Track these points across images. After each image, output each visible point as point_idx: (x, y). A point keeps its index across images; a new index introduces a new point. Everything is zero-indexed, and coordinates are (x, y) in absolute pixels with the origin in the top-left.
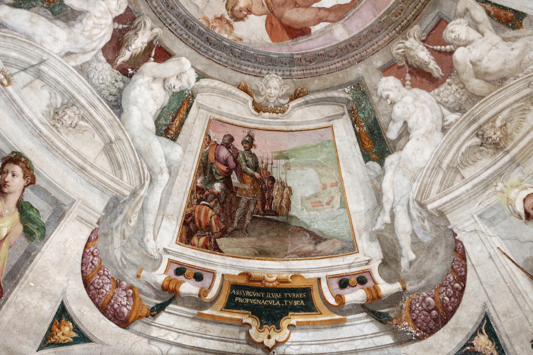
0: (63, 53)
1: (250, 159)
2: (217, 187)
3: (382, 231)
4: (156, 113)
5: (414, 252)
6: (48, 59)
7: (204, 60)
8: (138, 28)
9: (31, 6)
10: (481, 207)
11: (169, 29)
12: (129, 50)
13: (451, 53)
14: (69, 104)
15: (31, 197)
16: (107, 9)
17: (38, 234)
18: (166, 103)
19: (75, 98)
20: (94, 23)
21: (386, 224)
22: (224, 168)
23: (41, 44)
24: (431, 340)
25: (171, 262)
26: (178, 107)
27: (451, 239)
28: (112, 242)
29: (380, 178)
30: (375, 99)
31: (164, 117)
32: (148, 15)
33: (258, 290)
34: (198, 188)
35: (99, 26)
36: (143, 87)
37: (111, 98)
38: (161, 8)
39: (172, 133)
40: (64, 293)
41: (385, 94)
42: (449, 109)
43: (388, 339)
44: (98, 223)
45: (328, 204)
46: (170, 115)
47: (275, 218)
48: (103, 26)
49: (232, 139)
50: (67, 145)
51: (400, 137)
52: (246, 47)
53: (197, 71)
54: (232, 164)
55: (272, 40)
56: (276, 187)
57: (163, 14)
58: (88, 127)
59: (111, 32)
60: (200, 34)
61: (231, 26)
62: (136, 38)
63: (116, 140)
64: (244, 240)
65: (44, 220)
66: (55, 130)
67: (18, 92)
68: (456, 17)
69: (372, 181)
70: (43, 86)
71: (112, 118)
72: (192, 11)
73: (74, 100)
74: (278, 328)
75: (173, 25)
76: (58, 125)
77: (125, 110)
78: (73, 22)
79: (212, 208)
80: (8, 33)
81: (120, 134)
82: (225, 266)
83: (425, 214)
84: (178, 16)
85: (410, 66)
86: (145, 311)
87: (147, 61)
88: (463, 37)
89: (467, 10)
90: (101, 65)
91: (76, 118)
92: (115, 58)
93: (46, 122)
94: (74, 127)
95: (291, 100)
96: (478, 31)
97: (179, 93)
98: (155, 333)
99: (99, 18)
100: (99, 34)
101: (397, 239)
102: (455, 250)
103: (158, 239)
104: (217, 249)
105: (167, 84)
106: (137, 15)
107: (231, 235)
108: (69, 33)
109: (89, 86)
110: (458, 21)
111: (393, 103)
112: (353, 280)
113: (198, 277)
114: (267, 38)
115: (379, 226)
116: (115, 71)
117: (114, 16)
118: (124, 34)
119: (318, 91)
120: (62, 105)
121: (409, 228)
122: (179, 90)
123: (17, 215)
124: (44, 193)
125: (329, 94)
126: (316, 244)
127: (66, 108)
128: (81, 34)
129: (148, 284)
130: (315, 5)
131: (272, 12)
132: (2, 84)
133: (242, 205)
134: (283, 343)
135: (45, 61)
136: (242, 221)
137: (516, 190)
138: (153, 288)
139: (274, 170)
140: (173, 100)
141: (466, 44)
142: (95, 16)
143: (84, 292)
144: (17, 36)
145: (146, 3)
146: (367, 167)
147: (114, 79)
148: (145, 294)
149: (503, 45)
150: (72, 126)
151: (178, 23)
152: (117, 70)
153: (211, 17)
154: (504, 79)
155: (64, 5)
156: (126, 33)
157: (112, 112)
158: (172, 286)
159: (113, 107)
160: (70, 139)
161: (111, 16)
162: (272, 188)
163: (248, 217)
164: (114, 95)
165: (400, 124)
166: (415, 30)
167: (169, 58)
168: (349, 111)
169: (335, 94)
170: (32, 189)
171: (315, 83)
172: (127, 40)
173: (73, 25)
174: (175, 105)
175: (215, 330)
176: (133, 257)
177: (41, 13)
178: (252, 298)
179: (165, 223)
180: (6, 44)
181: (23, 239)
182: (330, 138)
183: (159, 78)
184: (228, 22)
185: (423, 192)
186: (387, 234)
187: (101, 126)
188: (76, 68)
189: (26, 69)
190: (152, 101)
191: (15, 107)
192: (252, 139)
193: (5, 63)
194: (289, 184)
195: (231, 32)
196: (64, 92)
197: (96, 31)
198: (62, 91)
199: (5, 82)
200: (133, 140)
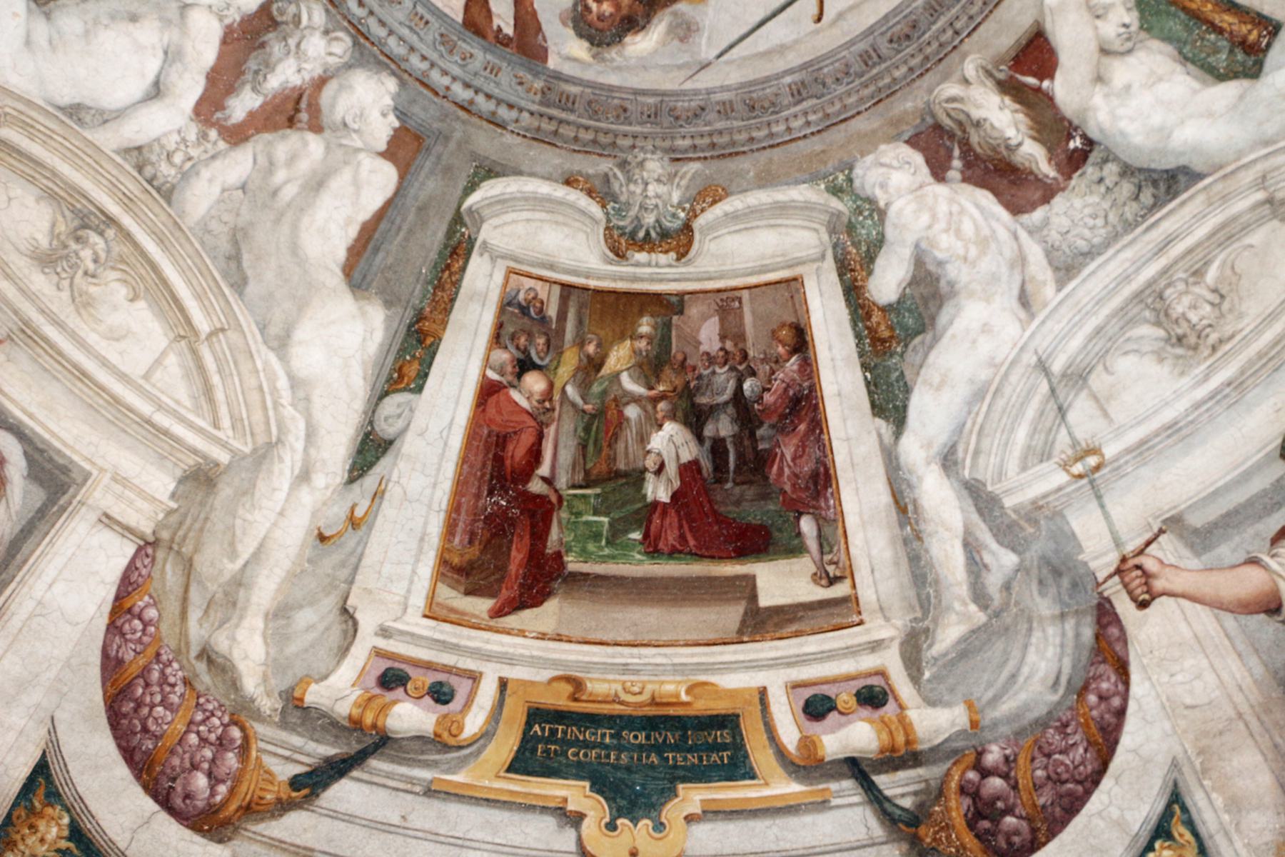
0: (1022, 314)
4: (1196, 78)
6: (1036, 352)
8: (962, 117)
9: (901, 383)
11: (969, 35)
12: (1020, 144)
14: (1158, 306)
16: (910, 197)
18: (1169, 49)
19: (1142, 291)
20: (947, 231)
23: (998, 367)
26: (1182, 15)
31: (1208, 55)
32: (930, 91)
35: (955, 218)
36: (1121, 111)
37: (1147, 197)
38: (913, 56)
39: (1255, 33)
46: (1203, 39)
48: (955, 208)
57: (928, 50)
58: (1224, 262)
59: (969, 189)
62: (987, 125)
63: (1265, 189)
66: (1227, 347)
67: (1119, 432)
70: (1106, 368)
71: (1201, 198)
73: (1147, 292)
75: (958, 25)
76: (1213, 337)
77: (1182, 161)
78: (943, 283)
80: (968, 444)
81: (1248, 177)
87: (1051, 99)
90: (1055, 220)
91: (1197, 289)
92: (1038, 181)
93: (1203, 367)
94: (1222, 297)
97: (1142, 12)
99: (934, 217)
100: (972, 217)
105: (1117, 46)
106: (930, 120)
108: (971, 295)
109: (1110, 252)
116: (1073, 182)
117: (930, 179)
118: (977, 156)
120: (1158, 324)
122: (1135, 14)
127: (1167, 315)
128: (973, 264)
132: (1098, 468)
135: (1040, 360)
140: (1162, 30)
142: (930, 227)
144: (974, 423)
145: (899, 94)
147: (1094, 187)
150: (1217, 300)
151: (954, 11)
152: (1070, 178)
155: (899, 302)
156: (975, 152)
157: (1185, 196)
159: (1172, 193)
160: (1253, 310)
161: (929, 188)
164: (1140, 188)
167: (1046, 40)
172: (994, 149)
173: (951, 284)
174: (1175, 25)
177: (918, 359)
180: (994, 450)
183: (1099, 63)
187: (1223, 226)
188: (1060, 285)
189: (1060, 408)
190: (1163, 88)
191: (1160, 442)
193: (1045, 456)
196: (1125, 317)
197: (968, 227)
198: (1121, 323)
199: (1092, 461)
200: (1267, 143)
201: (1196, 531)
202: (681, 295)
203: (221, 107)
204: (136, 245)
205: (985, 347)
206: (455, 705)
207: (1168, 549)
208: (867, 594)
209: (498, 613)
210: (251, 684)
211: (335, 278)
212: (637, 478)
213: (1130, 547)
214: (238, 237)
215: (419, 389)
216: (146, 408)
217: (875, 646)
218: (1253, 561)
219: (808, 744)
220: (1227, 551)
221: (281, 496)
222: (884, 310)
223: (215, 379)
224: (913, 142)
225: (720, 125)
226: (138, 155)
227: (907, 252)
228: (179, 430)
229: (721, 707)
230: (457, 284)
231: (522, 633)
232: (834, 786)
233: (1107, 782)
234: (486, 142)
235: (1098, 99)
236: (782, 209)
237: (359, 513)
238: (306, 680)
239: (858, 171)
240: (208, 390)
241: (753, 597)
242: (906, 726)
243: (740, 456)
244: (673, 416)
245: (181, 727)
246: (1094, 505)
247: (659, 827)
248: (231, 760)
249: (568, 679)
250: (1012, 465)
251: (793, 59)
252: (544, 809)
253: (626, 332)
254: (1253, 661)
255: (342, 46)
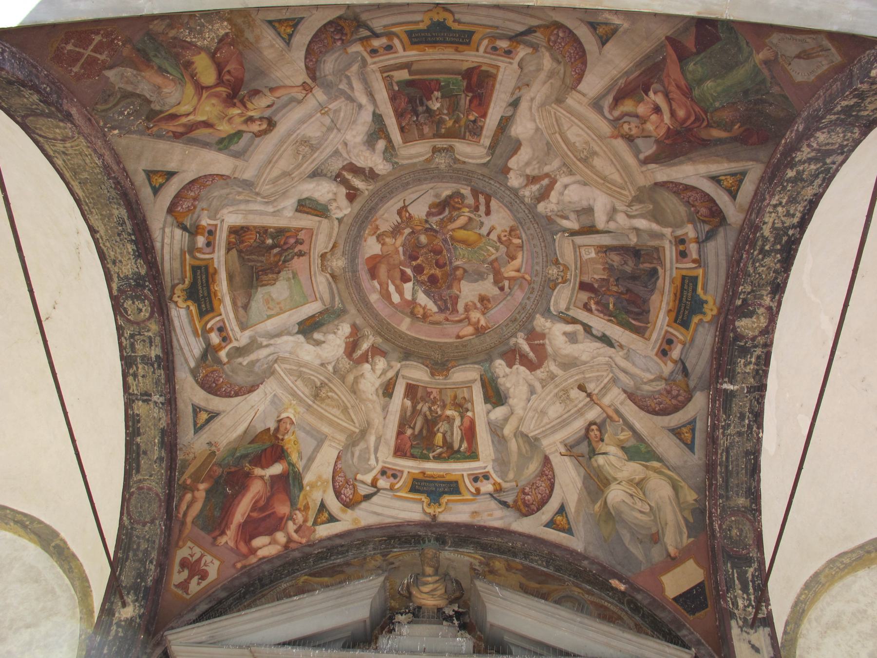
1: (290, 257)
2: (269, 241)
3: (257, 342)
5: (247, 364)
7: (350, 221)
10: (281, 394)
13: (367, 362)
15: (246, 138)
17: (221, 146)
21: (261, 343)
22: (282, 243)
24: (198, 388)
25: (216, 226)
27: (259, 382)
28: (223, 189)
29: (289, 334)
30: (336, 322)
33: (207, 281)
34: (266, 230)
37: (319, 171)
40: (184, 171)
41: (340, 327)
42: (335, 365)
43: (192, 364)
44: (235, 178)
45: (268, 308)
47: (255, 279)
49: (301, 244)
50: (284, 151)
51: (315, 340)
52: (360, 244)
53: (343, 218)
54: (285, 247)
55: (368, 258)
56: (275, 276)
59: (363, 166)
60: (367, 218)
61: (373, 235)
64: (237, 264)
65: (232, 148)
68: (388, 361)
69: (286, 329)
72: (381, 212)
74: (186, 300)
76: (297, 144)
79: (255, 241)
81: (296, 179)
82: (219, 258)
83: (271, 364)
84: (377, 204)
85: (358, 340)
86: (180, 220)
88: (377, 367)
89: (392, 367)
95: (330, 274)
96: (381, 375)
98: (168, 230)
99: (371, 159)
101: (253, 352)
102: (253, 386)
103: (230, 215)
104: (228, 250)
107: (240, 256)
110: (386, 363)
111: (335, 333)
112: (224, 334)
113: (208, 244)
114: (367, 256)
115: (259, 339)
119: (338, 289)
121: (261, 357)
123: (233, 132)
124: (250, 143)
125: (336, 296)
126: (242, 307)
129: (199, 217)
130: (389, 281)
131: (384, 257)
133: (260, 258)
134: (177, 306)
136: (249, 260)
137: (293, 412)
138: (196, 221)
139: (285, 272)
141: (373, 370)
143: (187, 182)
146: (294, 325)
148: (192, 216)
149: (374, 389)
153: (377, 223)
154: (355, 393)
158: (200, 231)
159: (314, 172)
162: (273, 273)
163: (252, 264)
165: (323, 339)
166: (379, 340)
168: (327, 309)
169: (337, 299)
170: (252, 137)
171: (342, 286)
173: (365, 145)
174: (319, 207)
175: (177, 265)
176: (215, 203)
178: (201, 280)
179: (240, 216)
181: (217, 139)
182: (310, 300)
184: (375, 233)
185: (284, 360)
186: (255, 345)
188: (337, 149)
192: (303, 255)
194: (277, 283)
195: (369, 235)
197: (362, 158)
199: (323, 112)
201: (294, 101)
202: (434, 138)
203: (551, 182)
204: (573, 154)
205: (354, 133)
206: (491, 46)
207: (300, 96)
208: (378, 75)
209: (479, 67)
210: (547, 54)
211: (524, 143)
212: (442, 97)
213: (310, 95)
214: (548, 154)
215: (502, 117)
216: (573, 118)
217: (375, 63)
218: (278, 98)
219: (390, 39)
220: (286, 98)
221: (539, 95)
222: (381, 138)
223: (555, 123)
224: (378, 175)
225: (427, 176)
226: (571, 173)
227: (377, 151)
228: (564, 113)
229: (416, 46)
230: (492, 140)
231: (473, 62)
232: (382, 31)
233: (307, 42)
234: (485, 171)
235: (335, 190)
236: (410, 158)
237: (518, 90)
238: (532, 54)
239: (391, 168)
240: (557, 121)
241: (409, 71)
242: (363, 46)
243: (416, 102)
244: (435, 111)
245: (566, 47)
246: (321, 102)
247: (431, 19)
248: (553, 38)
249: (459, 52)
250: (343, 107)
251: (410, 191)
252: (464, 23)
253: (448, 130)
254: (274, 77)
255: (521, 193)
